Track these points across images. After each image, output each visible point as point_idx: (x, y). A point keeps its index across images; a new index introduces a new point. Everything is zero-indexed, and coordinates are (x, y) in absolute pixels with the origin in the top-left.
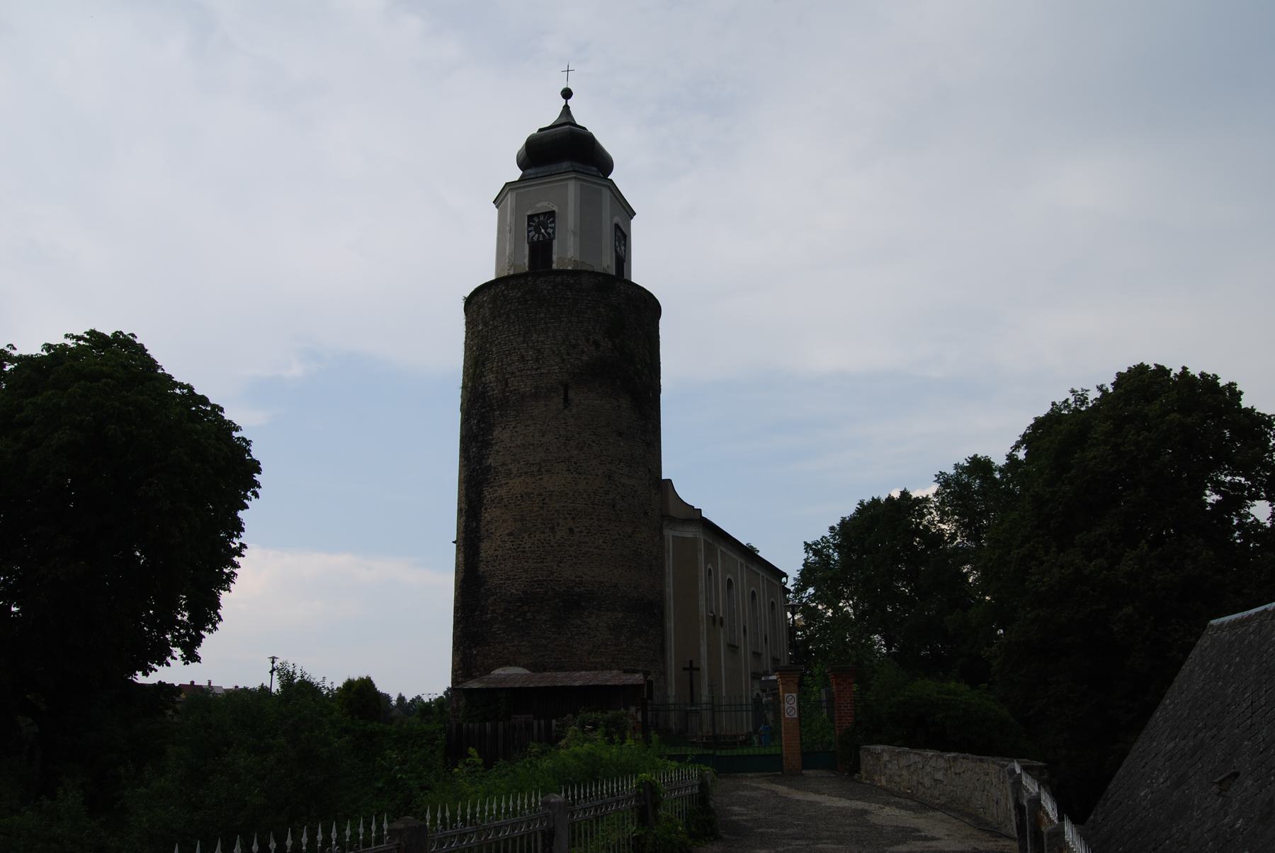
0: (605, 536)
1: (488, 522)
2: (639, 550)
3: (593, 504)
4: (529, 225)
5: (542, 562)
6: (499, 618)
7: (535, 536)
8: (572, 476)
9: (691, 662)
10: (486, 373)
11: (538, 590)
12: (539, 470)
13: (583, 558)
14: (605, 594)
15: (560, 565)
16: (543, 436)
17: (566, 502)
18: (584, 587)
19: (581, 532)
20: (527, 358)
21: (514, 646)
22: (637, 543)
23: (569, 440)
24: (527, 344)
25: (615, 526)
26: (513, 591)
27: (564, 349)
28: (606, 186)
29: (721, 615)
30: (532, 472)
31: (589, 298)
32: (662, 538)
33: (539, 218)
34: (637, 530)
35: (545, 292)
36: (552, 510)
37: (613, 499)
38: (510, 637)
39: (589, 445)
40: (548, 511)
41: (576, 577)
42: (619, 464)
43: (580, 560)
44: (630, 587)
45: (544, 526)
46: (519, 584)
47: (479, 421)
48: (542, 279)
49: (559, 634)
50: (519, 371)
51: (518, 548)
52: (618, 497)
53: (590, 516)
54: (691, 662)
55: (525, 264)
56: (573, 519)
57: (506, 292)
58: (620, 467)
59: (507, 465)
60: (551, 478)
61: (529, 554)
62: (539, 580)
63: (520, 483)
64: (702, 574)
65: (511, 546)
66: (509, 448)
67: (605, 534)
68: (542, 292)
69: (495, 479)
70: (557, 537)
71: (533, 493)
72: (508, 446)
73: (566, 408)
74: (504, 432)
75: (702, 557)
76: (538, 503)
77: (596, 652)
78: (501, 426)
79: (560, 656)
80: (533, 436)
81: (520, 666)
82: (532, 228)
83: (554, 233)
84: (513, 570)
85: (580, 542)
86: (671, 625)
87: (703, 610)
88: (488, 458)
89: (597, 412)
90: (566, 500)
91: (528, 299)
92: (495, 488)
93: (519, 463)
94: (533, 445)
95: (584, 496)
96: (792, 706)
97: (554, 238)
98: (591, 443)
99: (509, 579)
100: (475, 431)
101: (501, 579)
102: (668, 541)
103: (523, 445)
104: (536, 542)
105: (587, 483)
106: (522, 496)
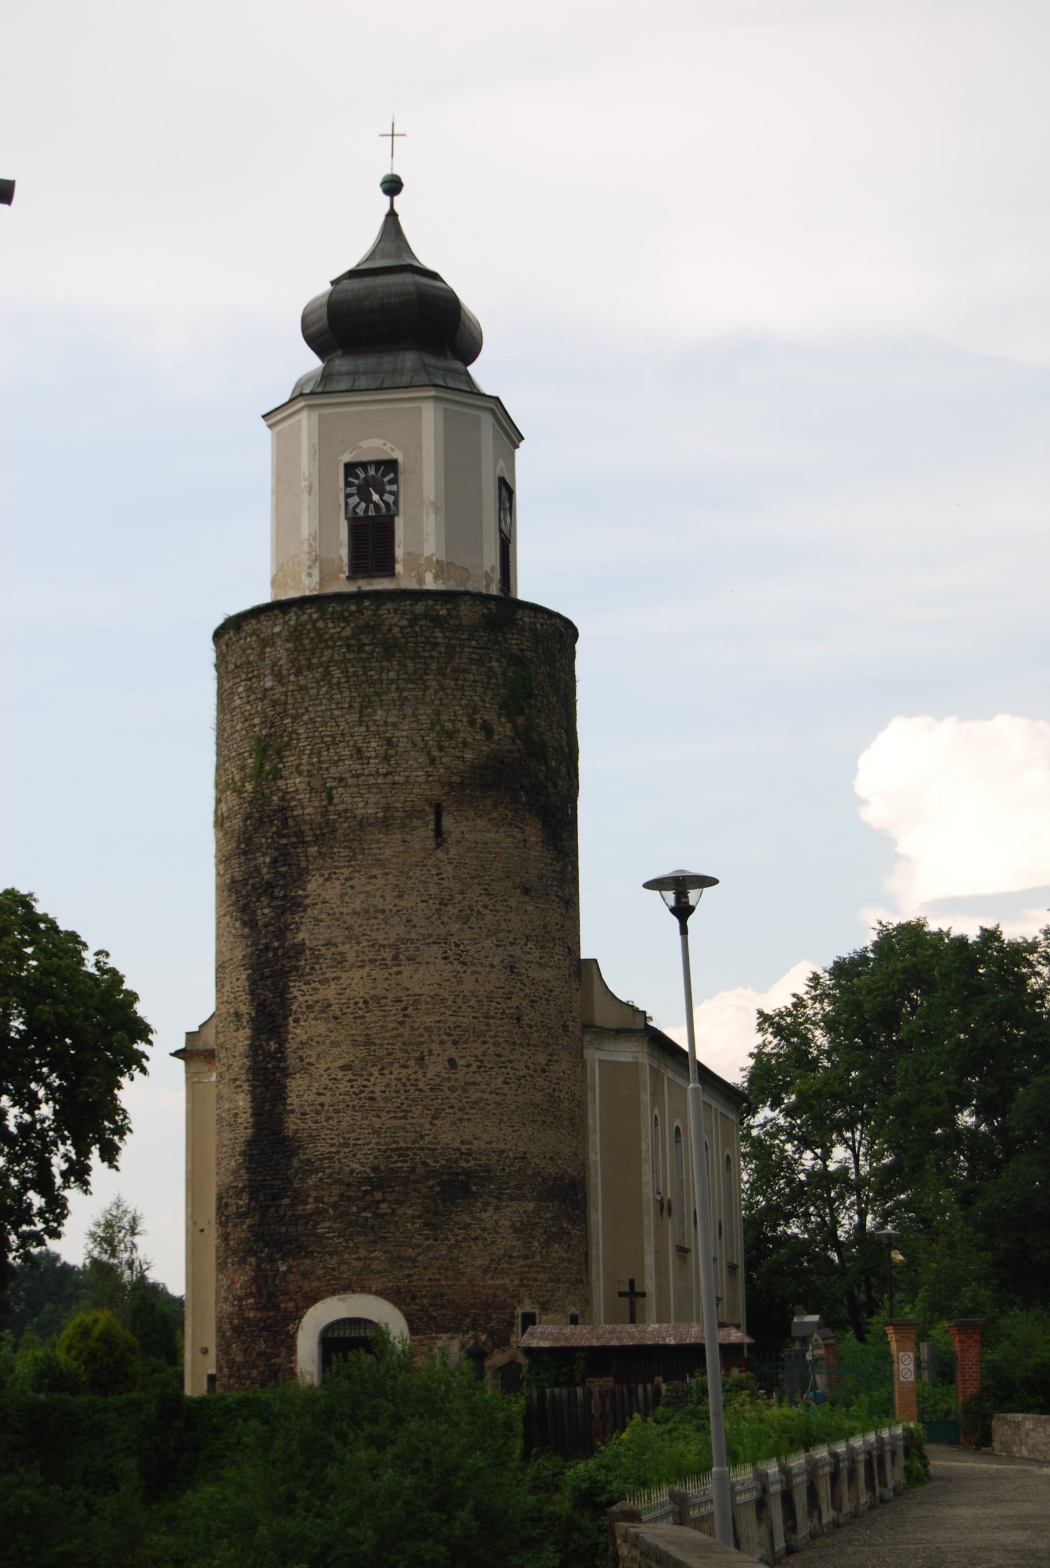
0: (506, 1071)
1: (301, 1043)
2: (557, 1094)
3: (486, 1017)
4: (348, 484)
5: (405, 1118)
6: (331, 1211)
7: (391, 1073)
8: (452, 969)
9: (632, 1282)
10: (286, 773)
11: (399, 1165)
12: (395, 957)
13: (473, 1111)
14: (507, 1170)
15: (435, 1122)
16: (401, 896)
17: (442, 1014)
18: (475, 1159)
19: (468, 1066)
20: (369, 754)
21: (359, 1259)
22: (555, 1081)
23: (446, 905)
24: (367, 727)
25: (522, 1054)
26: (354, 1166)
27: (433, 740)
28: (492, 410)
29: (669, 1196)
30: (384, 959)
31: (474, 643)
32: (583, 1063)
33: (366, 471)
34: (555, 1058)
35: (396, 630)
36: (419, 1028)
37: (517, 1008)
38: (351, 1244)
39: (478, 911)
40: (412, 1028)
41: (462, 1143)
42: (526, 945)
43: (467, 1113)
44: (545, 1157)
45: (406, 1055)
46: (366, 1154)
47: (275, 861)
48: (389, 605)
49: (436, 1240)
50: (353, 776)
51: (362, 1092)
52: (525, 1003)
53: (482, 1039)
54: (632, 1282)
55: (341, 558)
56: (455, 1043)
57: (320, 624)
58: (527, 949)
59: (336, 945)
60: (416, 971)
61: (382, 1104)
62: (400, 1149)
63: (362, 978)
64: (647, 1126)
65: (348, 1089)
66: (338, 915)
67: (506, 1067)
68: (390, 630)
69: (313, 968)
70: (430, 1075)
71: (385, 998)
72: (337, 910)
73: (439, 846)
74: (328, 883)
75: (646, 1098)
76: (396, 1015)
77: (496, 1269)
78: (322, 875)
79: (437, 1276)
80: (382, 896)
81: (370, 1293)
82: (354, 490)
83: (396, 503)
84: (354, 1131)
85: (467, 1084)
86: (597, 1217)
87: (648, 1193)
88: (298, 929)
89: (489, 853)
90: (442, 1010)
91: (366, 641)
92: (313, 985)
93: (359, 943)
94: (383, 911)
95: (472, 1003)
96: (908, 1367)
97: (397, 514)
98: (481, 909)
99: (347, 1145)
100: (267, 877)
101: (333, 1145)
102: (593, 1071)
103: (367, 912)
104: (394, 1083)
105: (477, 981)
106: (366, 1002)
